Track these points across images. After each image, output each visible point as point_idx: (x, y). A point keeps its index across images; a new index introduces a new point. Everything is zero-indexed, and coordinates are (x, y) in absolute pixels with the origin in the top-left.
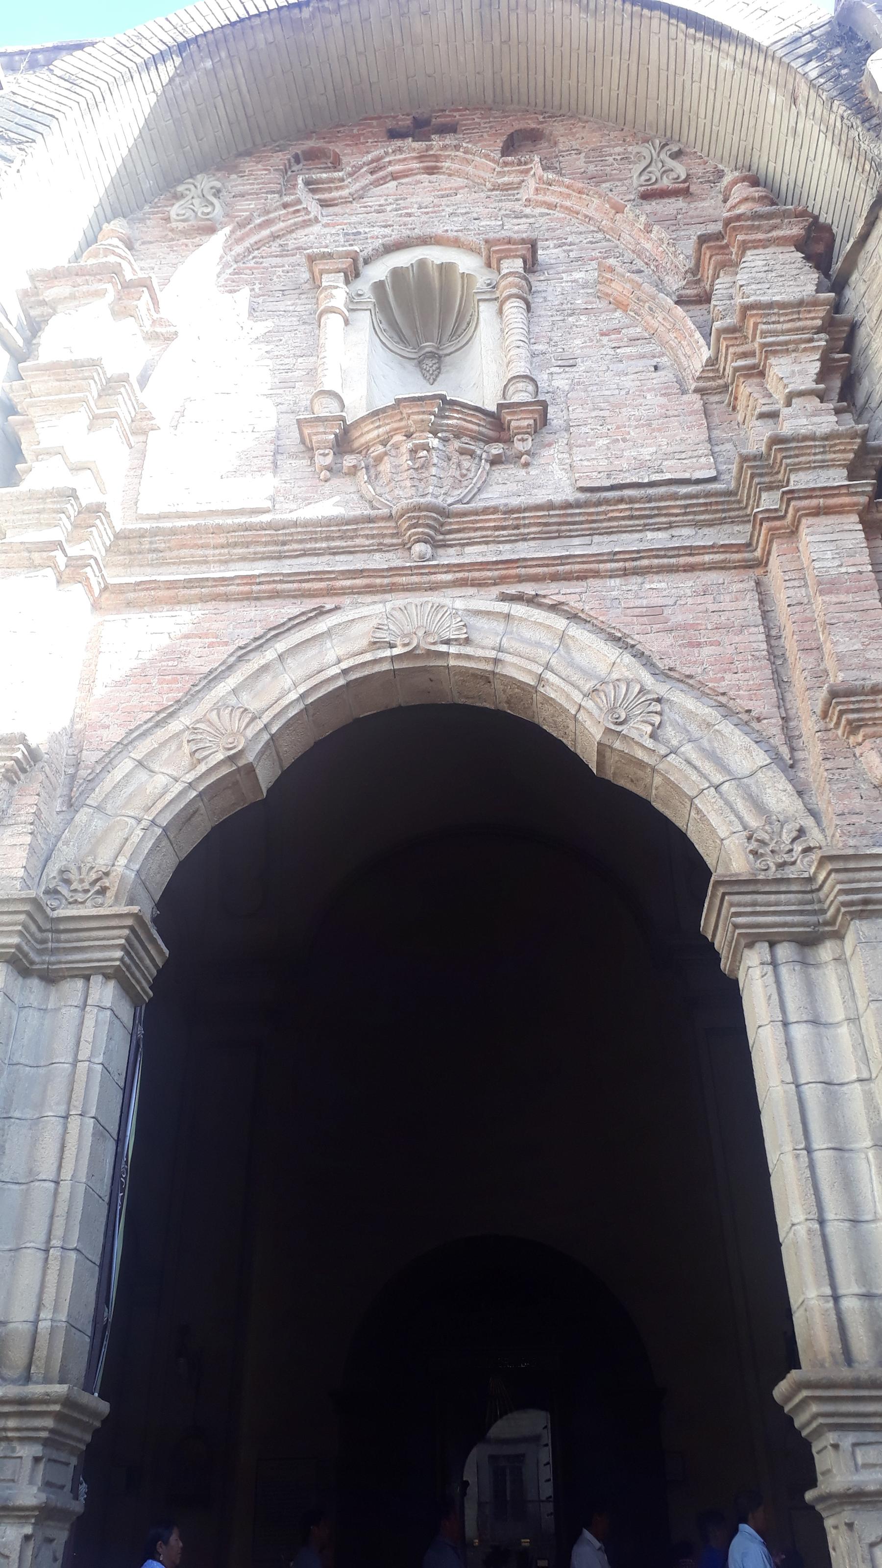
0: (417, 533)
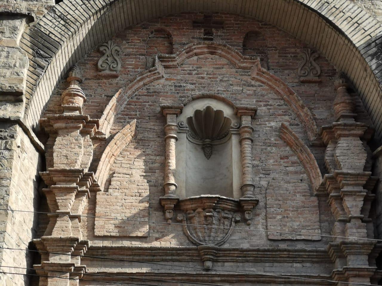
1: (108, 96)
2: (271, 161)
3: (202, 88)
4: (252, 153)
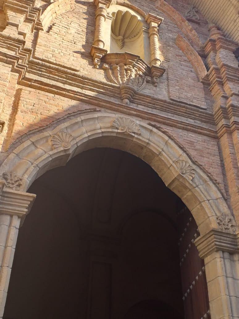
0: (127, 96)
2: (170, 55)
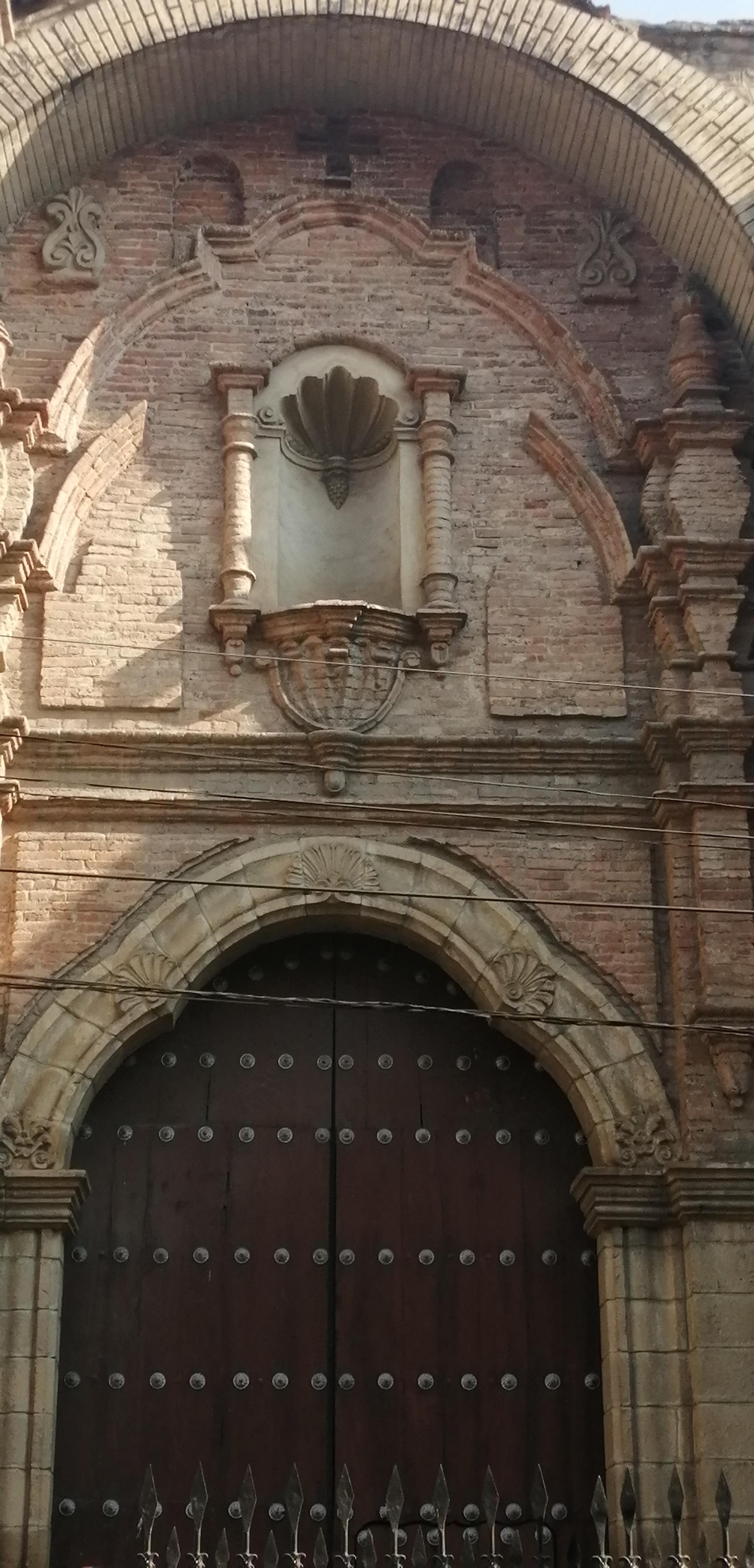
1: (70, 339)
2: (502, 513)
3: (321, 319)
4: (451, 492)
